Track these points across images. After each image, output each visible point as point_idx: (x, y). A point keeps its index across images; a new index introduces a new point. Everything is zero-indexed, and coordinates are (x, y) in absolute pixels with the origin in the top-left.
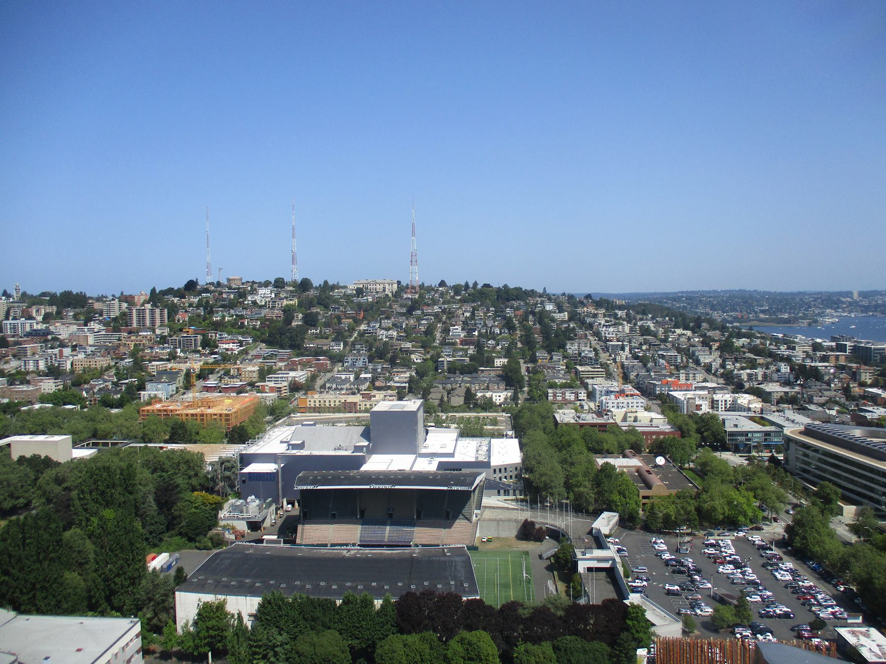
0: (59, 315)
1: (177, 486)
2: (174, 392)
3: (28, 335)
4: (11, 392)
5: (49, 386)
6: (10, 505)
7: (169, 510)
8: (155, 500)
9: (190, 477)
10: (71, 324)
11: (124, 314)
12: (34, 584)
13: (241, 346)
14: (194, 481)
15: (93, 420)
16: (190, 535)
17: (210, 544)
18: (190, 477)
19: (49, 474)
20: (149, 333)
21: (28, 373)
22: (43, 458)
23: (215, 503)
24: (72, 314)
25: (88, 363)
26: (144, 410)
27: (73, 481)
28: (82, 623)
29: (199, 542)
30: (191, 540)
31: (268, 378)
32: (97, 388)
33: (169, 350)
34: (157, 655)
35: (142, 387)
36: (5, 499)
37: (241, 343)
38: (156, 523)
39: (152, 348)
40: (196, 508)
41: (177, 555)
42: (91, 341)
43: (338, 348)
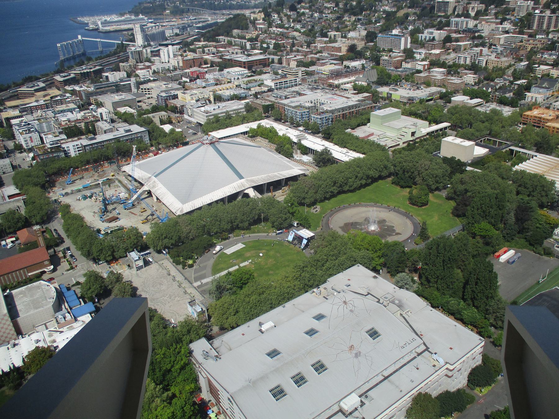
0: (485, 12)
1: (531, 208)
2: (550, 96)
3: (464, 31)
4: (448, 82)
5: (470, 78)
6: (436, 186)
7: (522, 223)
8: (515, 215)
9: (542, 196)
10: (491, 22)
11: (529, 15)
12: (438, 277)
14: (544, 200)
15: (491, 119)
16: (531, 242)
17: (542, 252)
18: (542, 196)
19: (458, 176)
20: (543, 36)
21: (459, 66)
22: (456, 159)
23: (554, 224)
24: (493, 12)
25: (497, 63)
26: (525, 115)
27: (470, 187)
28: (456, 326)
29: (536, 248)
30: (531, 244)
32: (499, 85)
33: (554, 57)
34: (492, 340)
35: (528, 88)
36: (433, 184)
38: (512, 229)
39: (543, 53)
40: (540, 224)
41: (520, 254)
42: (502, 42)
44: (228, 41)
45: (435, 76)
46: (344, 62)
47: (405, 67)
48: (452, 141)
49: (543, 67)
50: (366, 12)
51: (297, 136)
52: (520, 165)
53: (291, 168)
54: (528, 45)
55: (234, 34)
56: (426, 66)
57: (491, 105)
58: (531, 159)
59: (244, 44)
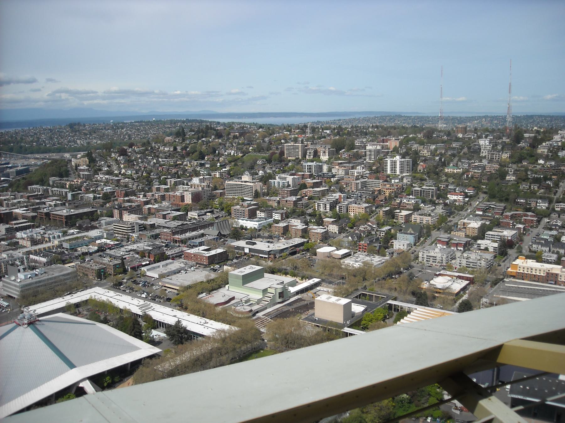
13: (465, 198)
31: (487, 234)
37: (466, 195)
43: (543, 205)
44: (44, 191)
45: (296, 226)
46: (189, 213)
47: (260, 216)
48: (326, 300)
49: (404, 213)
50: (209, 157)
51: (141, 307)
52: (402, 320)
53: (137, 348)
54: (385, 190)
55: (51, 183)
56: (284, 214)
57: (360, 256)
58: (412, 313)
59: (64, 194)
